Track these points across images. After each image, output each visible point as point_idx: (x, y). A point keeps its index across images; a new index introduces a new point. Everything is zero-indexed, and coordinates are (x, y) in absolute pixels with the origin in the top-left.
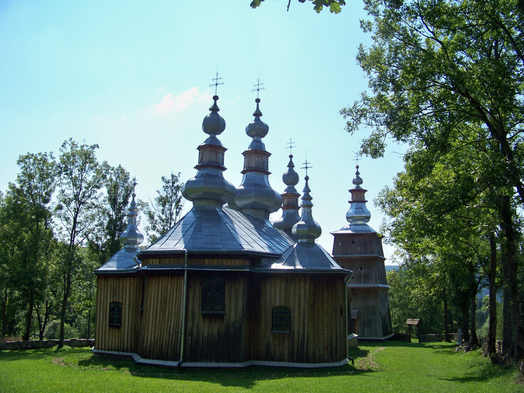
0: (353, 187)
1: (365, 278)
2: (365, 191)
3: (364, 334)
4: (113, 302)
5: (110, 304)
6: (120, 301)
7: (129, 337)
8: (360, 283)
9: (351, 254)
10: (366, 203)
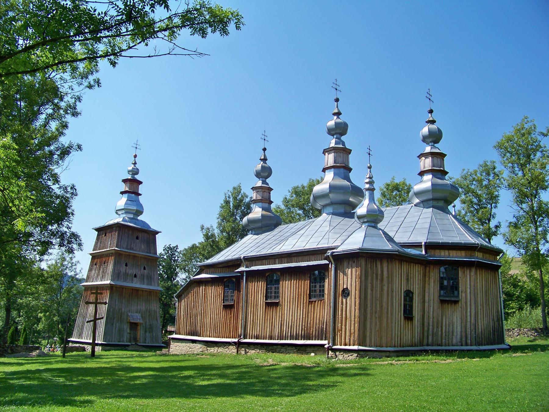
0: (130, 177)
1: (148, 279)
2: (140, 183)
3: (145, 339)
4: (405, 291)
5: (404, 292)
6: (412, 290)
7: (419, 330)
8: (144, 284)
9: (135, 251)
10: (140, 197)
